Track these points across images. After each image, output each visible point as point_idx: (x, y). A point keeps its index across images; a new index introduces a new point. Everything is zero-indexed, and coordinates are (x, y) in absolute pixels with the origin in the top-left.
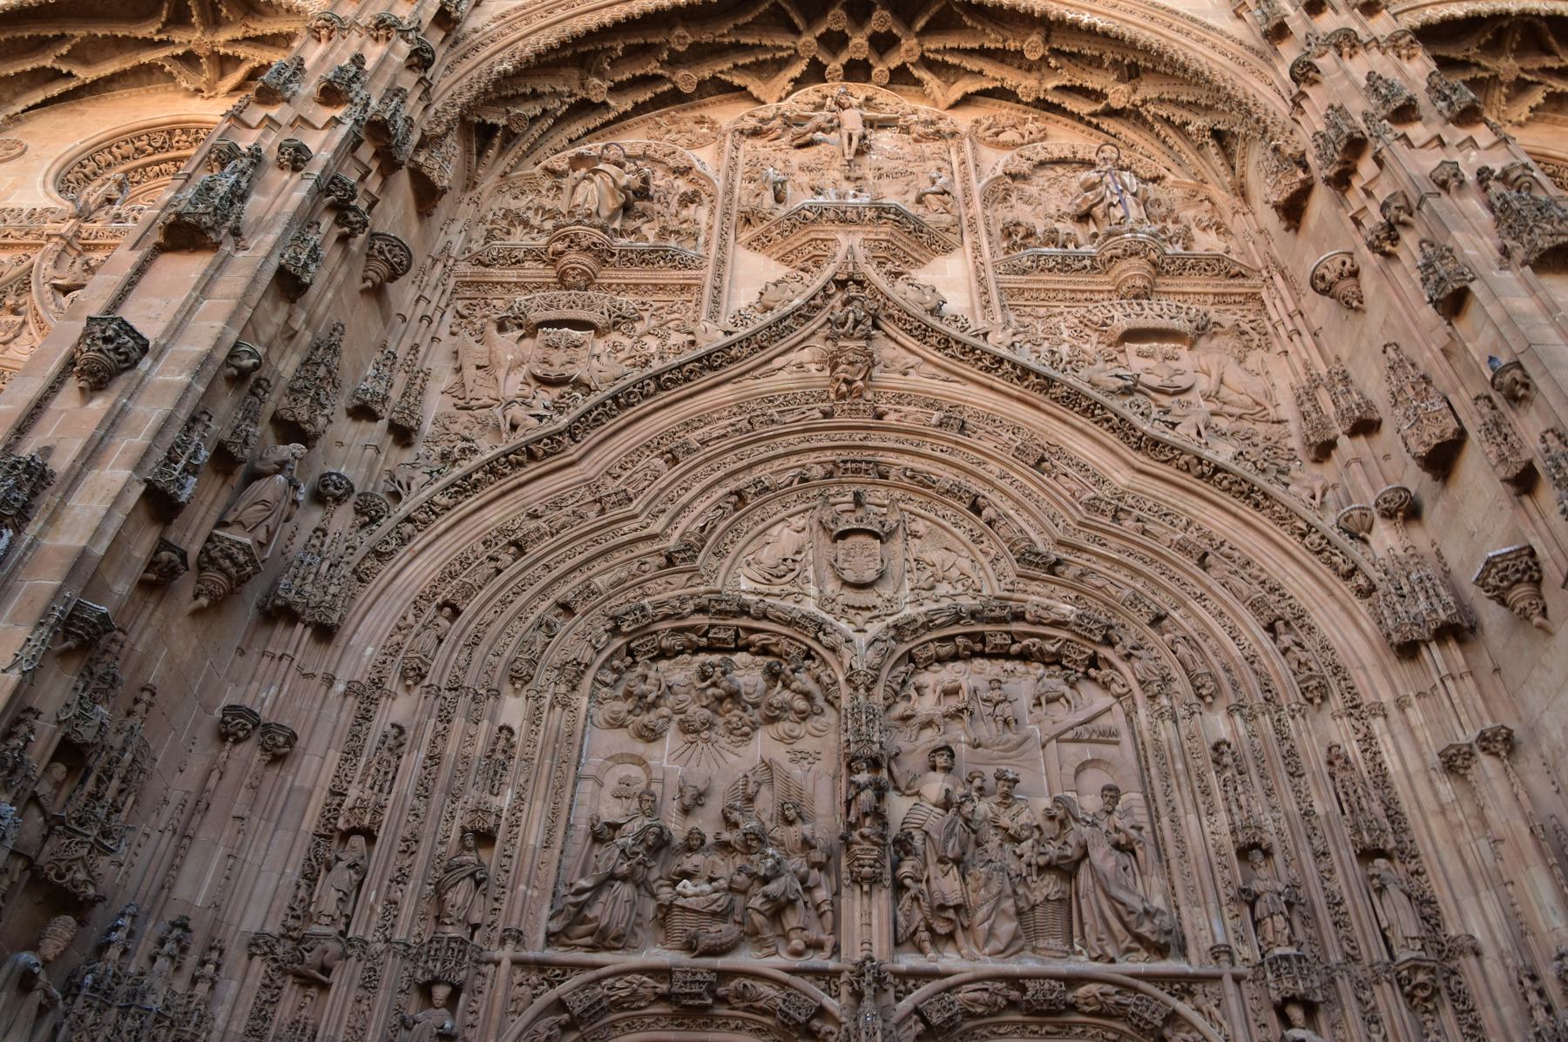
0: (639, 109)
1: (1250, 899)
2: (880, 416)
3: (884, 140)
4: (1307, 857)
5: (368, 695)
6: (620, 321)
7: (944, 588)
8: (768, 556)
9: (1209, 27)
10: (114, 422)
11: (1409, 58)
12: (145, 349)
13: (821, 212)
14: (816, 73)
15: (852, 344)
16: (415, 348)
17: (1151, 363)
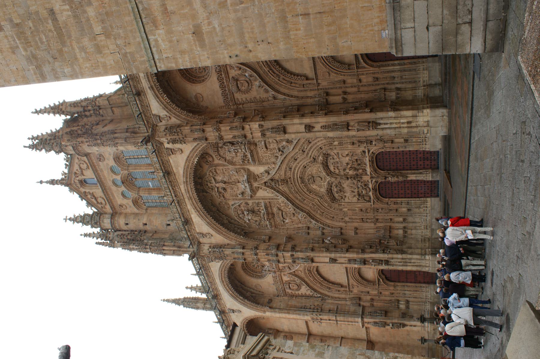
0: (223, 214)
1: (359, 146)
2: (290, 177)
3: (219, 178)
4: (353, 139)
5: (346, 222)
6: (280, 209)
7: (320, 170)
8: (318, 189)
9: (198, 144)
10: (341, 257)
11: (219, 128)
12: (330, 258)
13: (251, 190)
14: (204, 191)
15: (280, 184)
16: (294, 231)
17: (271, 144)
